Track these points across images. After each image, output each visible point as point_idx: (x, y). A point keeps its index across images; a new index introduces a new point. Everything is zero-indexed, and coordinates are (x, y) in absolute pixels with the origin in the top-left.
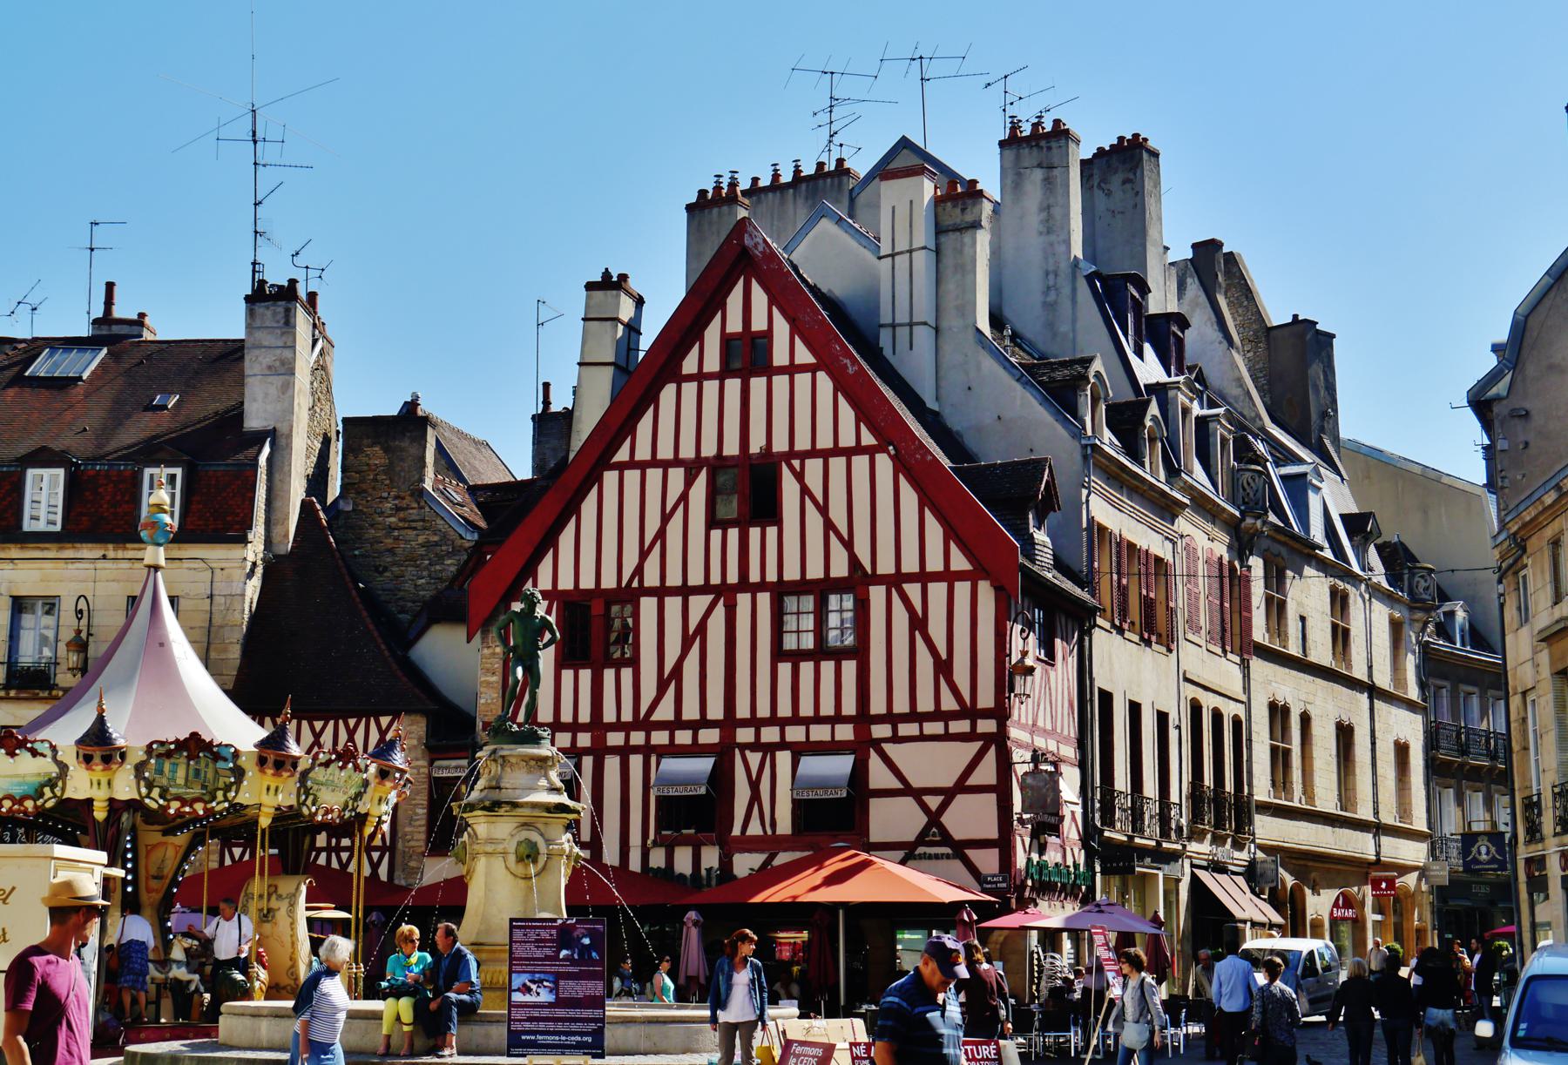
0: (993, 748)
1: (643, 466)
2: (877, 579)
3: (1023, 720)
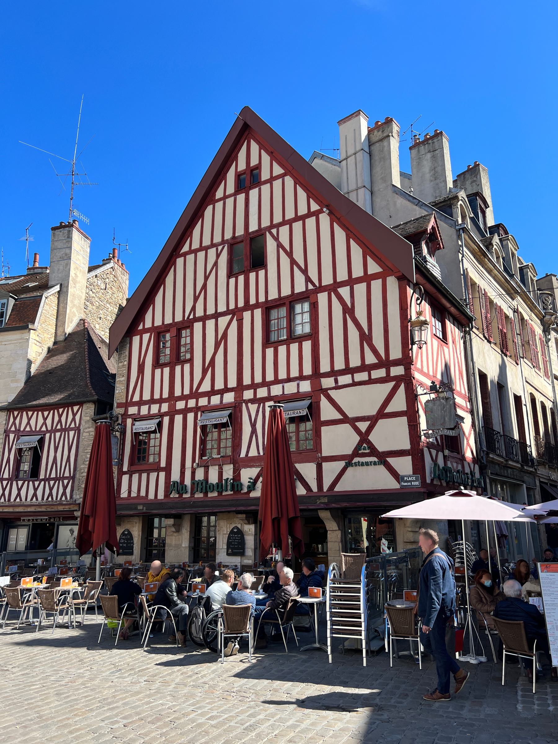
0: (403, 385)
1: (195, 252)
2: (321, 289)
3: (425, 370)
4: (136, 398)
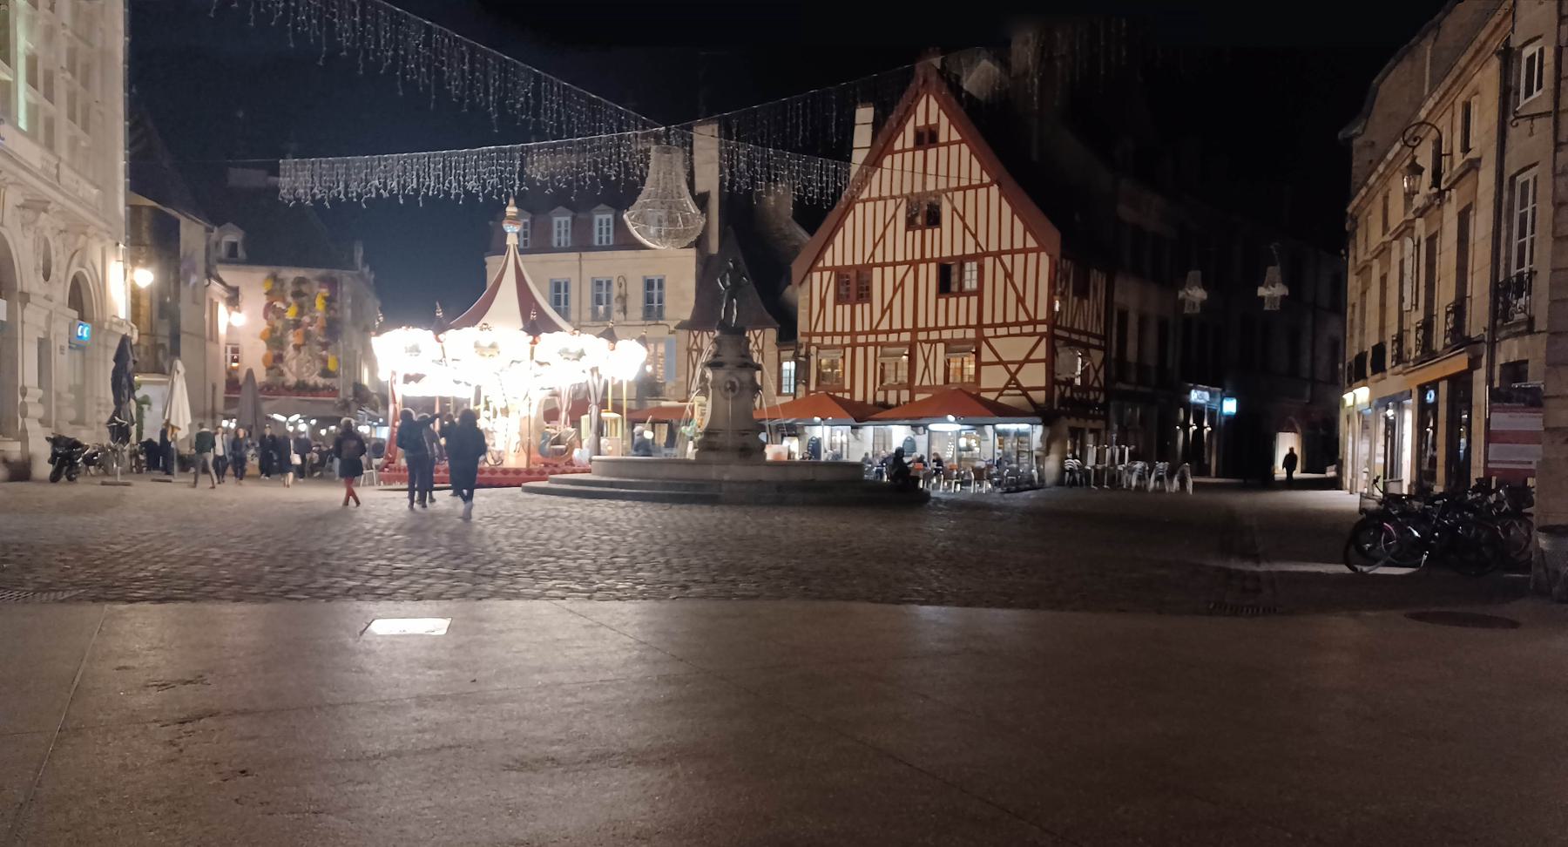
1: (875, 200)
2: (987, 254)
3: (1064, 324)
4: (819, 329)
